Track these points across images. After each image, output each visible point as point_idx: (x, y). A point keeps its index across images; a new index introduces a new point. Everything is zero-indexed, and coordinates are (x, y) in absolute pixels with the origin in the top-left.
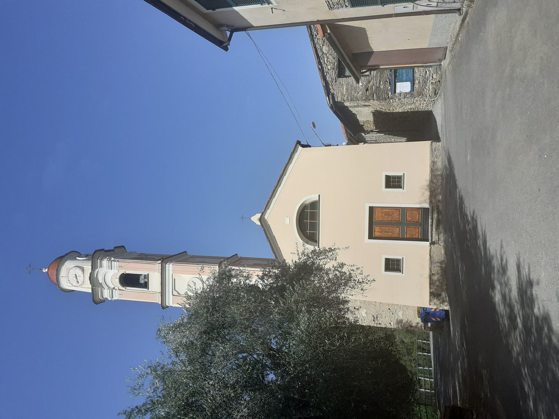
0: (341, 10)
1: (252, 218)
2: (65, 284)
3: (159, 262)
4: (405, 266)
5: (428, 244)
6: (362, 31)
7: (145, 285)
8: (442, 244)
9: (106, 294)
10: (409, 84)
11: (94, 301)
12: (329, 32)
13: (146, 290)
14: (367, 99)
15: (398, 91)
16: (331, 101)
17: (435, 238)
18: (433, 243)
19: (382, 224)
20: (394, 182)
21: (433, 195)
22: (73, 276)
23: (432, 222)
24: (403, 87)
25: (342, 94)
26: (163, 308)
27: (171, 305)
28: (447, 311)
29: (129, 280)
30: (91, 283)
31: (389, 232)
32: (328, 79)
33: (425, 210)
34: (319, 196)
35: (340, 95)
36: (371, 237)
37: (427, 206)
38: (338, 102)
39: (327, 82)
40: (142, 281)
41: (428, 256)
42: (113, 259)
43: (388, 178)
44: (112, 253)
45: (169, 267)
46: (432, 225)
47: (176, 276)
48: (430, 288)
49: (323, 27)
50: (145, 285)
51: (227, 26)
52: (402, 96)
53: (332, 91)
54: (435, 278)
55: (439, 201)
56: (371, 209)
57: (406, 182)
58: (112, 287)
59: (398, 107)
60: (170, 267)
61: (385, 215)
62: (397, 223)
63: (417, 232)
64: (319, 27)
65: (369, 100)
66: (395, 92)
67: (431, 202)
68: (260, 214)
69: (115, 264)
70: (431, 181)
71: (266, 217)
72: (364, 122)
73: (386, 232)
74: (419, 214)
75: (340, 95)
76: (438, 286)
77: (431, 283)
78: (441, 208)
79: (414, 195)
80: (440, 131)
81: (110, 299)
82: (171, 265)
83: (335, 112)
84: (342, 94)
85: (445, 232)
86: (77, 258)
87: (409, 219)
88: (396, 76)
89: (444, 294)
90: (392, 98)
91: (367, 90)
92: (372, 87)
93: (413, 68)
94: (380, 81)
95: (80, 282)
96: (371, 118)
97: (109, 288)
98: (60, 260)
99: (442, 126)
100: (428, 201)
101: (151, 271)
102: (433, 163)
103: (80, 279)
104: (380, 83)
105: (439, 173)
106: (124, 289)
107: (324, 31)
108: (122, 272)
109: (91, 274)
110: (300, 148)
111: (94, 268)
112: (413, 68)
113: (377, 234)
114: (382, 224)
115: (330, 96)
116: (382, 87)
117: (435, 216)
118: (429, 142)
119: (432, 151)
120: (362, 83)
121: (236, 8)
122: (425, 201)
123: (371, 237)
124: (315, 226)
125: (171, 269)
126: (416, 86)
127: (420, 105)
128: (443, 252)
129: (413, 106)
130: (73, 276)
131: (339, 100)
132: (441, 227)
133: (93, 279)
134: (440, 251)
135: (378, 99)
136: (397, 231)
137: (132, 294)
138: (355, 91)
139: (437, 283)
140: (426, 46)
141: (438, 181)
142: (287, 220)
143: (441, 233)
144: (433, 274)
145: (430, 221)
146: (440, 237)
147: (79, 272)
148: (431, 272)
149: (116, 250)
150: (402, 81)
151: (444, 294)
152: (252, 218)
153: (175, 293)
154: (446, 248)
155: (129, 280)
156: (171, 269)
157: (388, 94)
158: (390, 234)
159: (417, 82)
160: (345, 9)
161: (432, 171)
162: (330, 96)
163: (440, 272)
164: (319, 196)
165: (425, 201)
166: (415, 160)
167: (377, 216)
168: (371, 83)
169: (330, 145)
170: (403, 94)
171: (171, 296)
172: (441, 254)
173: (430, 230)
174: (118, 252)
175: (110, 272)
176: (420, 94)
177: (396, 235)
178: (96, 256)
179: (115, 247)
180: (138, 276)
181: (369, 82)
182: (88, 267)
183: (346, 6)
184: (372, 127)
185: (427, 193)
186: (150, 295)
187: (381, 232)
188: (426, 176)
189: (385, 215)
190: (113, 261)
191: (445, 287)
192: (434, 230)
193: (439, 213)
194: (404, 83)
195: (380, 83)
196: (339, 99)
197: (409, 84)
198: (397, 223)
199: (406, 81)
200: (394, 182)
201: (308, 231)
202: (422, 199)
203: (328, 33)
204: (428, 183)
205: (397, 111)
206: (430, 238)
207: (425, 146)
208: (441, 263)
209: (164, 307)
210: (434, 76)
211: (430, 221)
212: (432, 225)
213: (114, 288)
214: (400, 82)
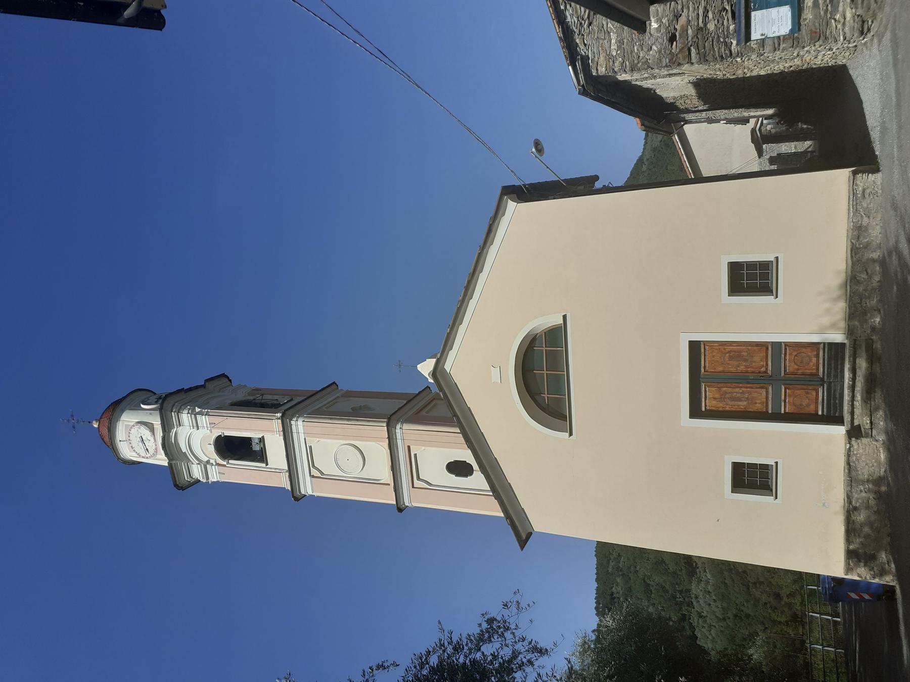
1: (420, 367)
2: (127, 452)
3: (279, 415)
5: (840, 431)
7: (261, 456)
8: (882, 437)
9: (197, 472)
11: (176, 486)
13: (264, 465)
14: (674, 62)
15: (755, 35)
16: (581, 76)
17: (862, 419)
18: (854, 433)
19: (724, 380)
20: (751, 279)
21: (856, 312)
22: (137, 438)
23: (854, 379)
24: (772, 22)
25: (609, 57)
27: (310, 493)
28: (890, 590)
29: (233, 448)
30: (166, 454)
31: (740, 400)
32: (569, 19)
33: (835, 350)
34: (565, 317)
35: (602, 58)
36: (696, 412)
37: (838, 337)
38: (598, 77)
39: (568, 27)
40: (256, 448)
42: (198, 410)
43: (735, 268)
44: (201, 392)
45: (297, 426)
46: (853, 388)
47: (313, 442)
52: (768, 48)
53: (582, 50)
54: (861, 517)
55: (873, 329)
56: (694, 347)
58: (205, 459)
59: (753, 67)
60: (299, 426)
61: (731, 358)
62: (762, 379)
65: (679, 64)
66: (748, 37)
68: (434, 360)
69: (203, 420)
71: (447, 367)
72: (674, 98)
73: (733, 399)
74: (817, 356)
75: (602, 58)
76: (867, 536)
77: (851, 530)
78: (878, 345)
79: (807, 313)
80: (875, 135)
81: (204, 481)
83: (596, 98)
84: (609, 57)
85: (893, 415)
86: (142, 406)
87: (791, 367)
89: (883, 556)
91: (672, 39)
92: (684, 30)
94: (706, 11)
95: (151, 451)
96: (691, 91)
97: (200, 461)
98: (115, 408)
99: (884, 130)
100: (842, 324)
102: (858, 231)
103: (151, 445)
104: (706, 16)
105: (875, 255)
108: (217, 433)
109: (164, 439)
110: (511, 206)
111: (166, 426)
113: (708, 401)
114: (724, 380)
115: (579, 65)
116: (711, 26)
117: (862, 364)
118: (843, 175)
119: (856, 197)
120: (659, 21)
122: (833, 326)
123: (696, 412)
125: (301, 430)
126: (808, 15)
127: (817, 56)
128: (883, 456)
129: (797, 62)
130: (137, 438)
131: (602, 71)
132: (878, 395)
133: (169, 446)
134: (874, 455)
135: (703, 59)
136: (760, 397)
137: (240, 472)
138: (641, 46)
139: (866, 530)
141: (870, 277)
142: (495, 373)
143: (877, 409)
144: (855, 509)
145: (847, 375)
146: (875, 421)
147: (146, 433)
148: (850, 502)
149: (210, 386)
150: (767, 7)
151: (883, 556)
152: (420, 367)
153: (315, 472)
154: (891, 445)
155: (233, 448)
156: (301, 430)
157: (728, 46)
158: (742, 405)
161: (856, 251)
162: (579, 65)
163: (872, 502)
164: (565, 317)
165: (833, 326)
168: (683, 20)
170: (769, 43)
171: (308, 478)
172: (878, 461)
175: (198, 433)
176: (820, 35)
177: (758, 407)
178: (169, 402)
179: (206, 381)
180: (250, 439)
181: (677, 17)
182: (157, 423)
184: (696, 102)
185: (842, 305)
186: (271, 473)
187: (721, 399)
188: (837, 262)
189: (731, 358)
190: (199, 413)
191: (886, 540)
192: (858, 397)
193: (872, 359)
195: (706, 16)
196: (601, 69)
198: (762, 379)
200: (751, 279)
201: (546, 396)
202: (826, 321)
204: (840, 279)
205: (755, 73)
206: (847, 417)
208: (878, 481)
209: (297, 497)
211: (847, 375)
212: (853, 388)
213: (208, 462)
214: (760, 8)
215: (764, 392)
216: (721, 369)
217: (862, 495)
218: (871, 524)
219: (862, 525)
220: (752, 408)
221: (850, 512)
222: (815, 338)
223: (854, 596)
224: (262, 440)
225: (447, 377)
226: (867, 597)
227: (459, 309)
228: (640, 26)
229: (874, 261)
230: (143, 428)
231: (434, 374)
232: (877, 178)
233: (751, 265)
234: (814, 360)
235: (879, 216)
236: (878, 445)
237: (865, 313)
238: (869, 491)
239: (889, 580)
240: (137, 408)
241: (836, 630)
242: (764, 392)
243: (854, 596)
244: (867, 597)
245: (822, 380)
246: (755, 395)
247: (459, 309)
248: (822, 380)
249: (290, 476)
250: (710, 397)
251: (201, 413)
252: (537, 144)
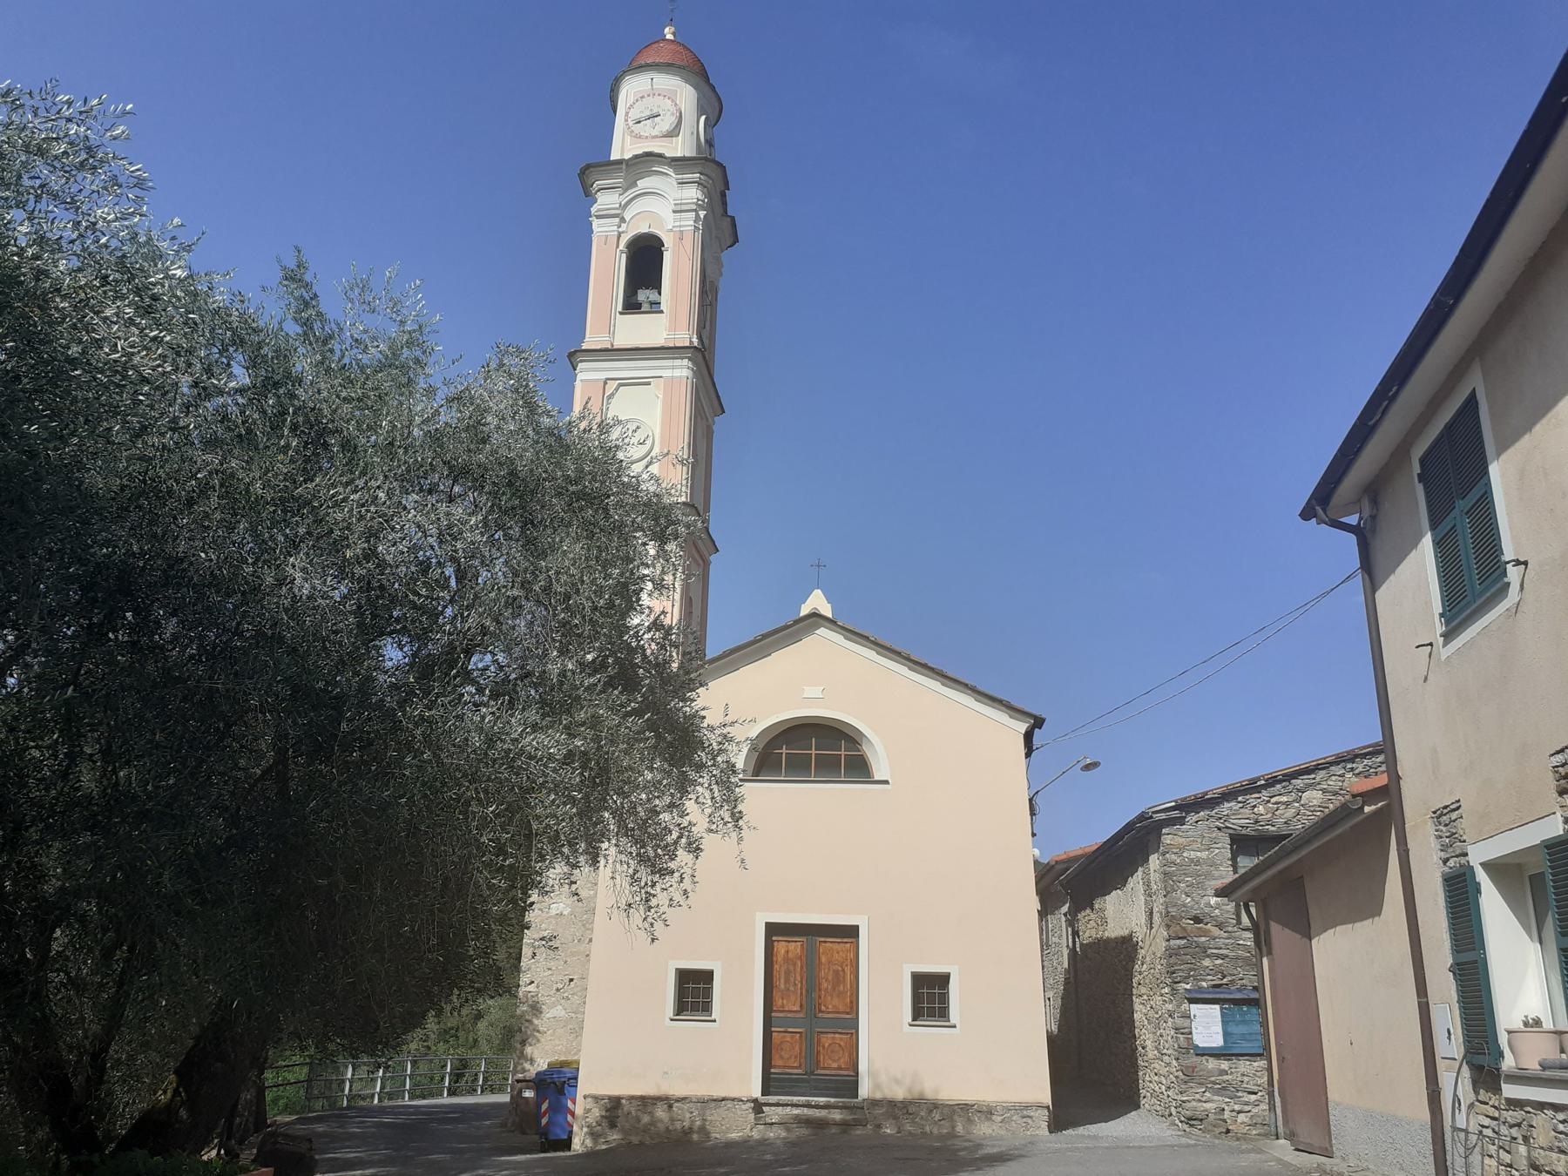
0: (1434, 844)
1: (818, 593)
2: (632, 88)
3: (695, 341)
4: (691, 1028)
5: (756, 1092)
6: (1370, 906)
7: (631, 306)
8: (756, 1134)
9: (606, 200)
10: (1217, 1041)
11: (588, 166)
12: (1367, 809)
13: (620, 308)
14: (1170, 920)
16: (1163, 816)
17: (773, 1114)
18: (758, 1107)
19: (811, 962)
20: (930, 996)
22: (654, 110)
23: (817, 1107)
24: (1208, 1026)
25: (1182, 848)
26: (571, 355)
27: (579, 377)
28: (566, 1144)
29: (645, 261)
30: (636, 157)
31: (787, 981)
32: (1227, 805)
33: (852, 1087)
34: (886, 782)
35: (1181, 840)
36: (773, 930)
37: (864, 1091)
38: (1160, 835)
39: (1218, 804)
40: (643, 295)
41: (723, 1095)
42: (702, 214)
43: (943, 980)
44: (719, 210)
45: (681, 367)
46: (808, 1106)
48: (632, 1098)
49: (1381, 792)
50: (631, 306)
51: (1373, 517)
52: (1180, 1022)
54: (661, 1112)
55: (879, 1126)
56: (851, 932)
57: (930, 1033)
58: (628, 215)
60: (682, 370)
61: (836, 973)
62: (812, 1008)
63: (790, 1062)
64: (1382, 780)
65: (1168, 926)
66: (1192, 1001)
67: (874, 1103)
68: (830, 615)
69: (688, 221)
70: (935, 1106)
71: (822, 631)
72: (1102, 910)
73: (788, 973)
74: (840, 1068)
75: (1181, 840)
76: (639, 1121)
77: (646, 1102)
78: (859, 1131)
79: (893, 1056)
80: (1081, 1130)
81: (593, 210)
82: (686, 373)
83: (1129, 827)
84: (1182, 848)
86: (703, 118)
87: (826, 1040)
88: (1239, 1004)
89: (615, 1137)
90: (1174, 991)
91: (1197, 920)
92: (1205, 933)
93: (1264, 1053)
94: (1223, 957)
95: (637, 128)
96: (1114, 931)
97: (624, 207)
98: (698, 73)
99: (1095, 1137)
100: (878, 1096)
101: (671, 319)
102: (988, 1112)
103: (646, 129)
104: (1218, 956)
105: (959, 1128)
106: (622, 247)
107: (1369, 796)
108: (668, 241)
109: (660, 156)
110: (1023, 727)
111: (678, 163)
112: (1264, 1053)
113: (781, 947)
114: (811, 962)
115: (1175, 814)
116: (1207, 962)
117: (837, 1115)
118: (1046, 1097)
119: (1023, 1109)
120: (1218, 906)
121: (1427, 542)
122: (877, 1086)
123: (773, 930)
124: (799, 769)
125: (677, 373)
126: (1212, 1064)
127: (1157, 1072)
128: (734, 1136)
129: (1152, 1053)
130: (654, 110)
131: (1167, 840)
132: (804, 1131)
133: (647, 161)
134: (736, 1127)
135: (1171, 953)
136: (790, 1004)
137: (607, 270)
138: (1191, 885)
139: (646, 1119)
140: (1334, 1094)
141: (936, 1123)
142: (815, 691)
143: (788, 1130)
144: (670, 1107)
145: (822, 1100)
146: (775, 1128)
147: (666, 123)
148: (677, 1101)
149: (726, 223)
150: (1224, 1023)
151: (615, 1137)
152: (818, 593)
153: (612, 386)
154: (744, 1145)
155: (645, 261)
156: (677, 373)
157: (1185, 980)
158: (781, 983)
159: (1225, 1065)
160: (1436, 856)
161: (965, 1107)
162: (1175, 814)
163: (678, 1125)
164: (886, 782)
165: (877, 1086)
166: (995, 1056)
167: (831, 948)
168: (1216, 932)
169: (1033, 814)
170: (1186, 1023)
171: (604, 375)
172: (729, 1130)
173: (795, 1099)
174: (720, 228)
175: (668, 209)
177: (778, 1002)
178: (711, 168)
179: (733, 219)
180: (657, 286)
181: (1220, 926)
182: (681, 147)
183: (1445, 861)
184: (1088, 933)
185: (899, 1094)
186: (606, 320)
187: (786, 959)
188: (950, 1090)
189: (836, 973)
190: (697, 216)
191: (635, 1140)
192: (796, 1111)
193: (845, 1126)
194: (1219, 1029)
195: (1218, 956)
197: (1217, 1041)
198: (812, 1008)
199: (1226, 1034)
200: (930, 996)
201: (784, 751)
202: (883, 1078)
203: (1362, 808)
204: (930, 1095)
205: (1137, 1007)
206: (773, 1099)
207: (1037, 1087)
208: (703, 1130)
209: (575, 356)
210: (1241, 1118)
211: (822, 1100)
212: (808, 1106)
213: (623, 220)
214: (1223, 1015)
215: (796, 1008)
216: (823, 960)
217: (686, 1117)
218: (653, 1123)
219: (651, 1114)
220: (777, 995)
221: (668, 1101)
222: (863, 1067)
223: (545, 1106)
224: (655, 307)
225: (810, 630)
226: (544, 1121)
227: (898, 654)
228: (1222, 892)
229: (953, 1127)
230: (673, 120)
231: (815, 615)
232: (1044, 1130)
233: (944, 998)
234: (835, 1065)
235: (1003, 1132)
236: (747, 1131)
237: (896, 1118)
238: (693, 1122)
239: (580, 1143)
240: (701, 110)
241: (364, 1099)
242: (796, 1008)
243: (545, 1106)
244: (544, 1121)
245: (812, 1073)
246: (792, 998)
247: (898, 654)
248: (812, 1073)
249: (606, 350)
250: (788, 948)
251: (697, 218)
252: (1095, 765)
